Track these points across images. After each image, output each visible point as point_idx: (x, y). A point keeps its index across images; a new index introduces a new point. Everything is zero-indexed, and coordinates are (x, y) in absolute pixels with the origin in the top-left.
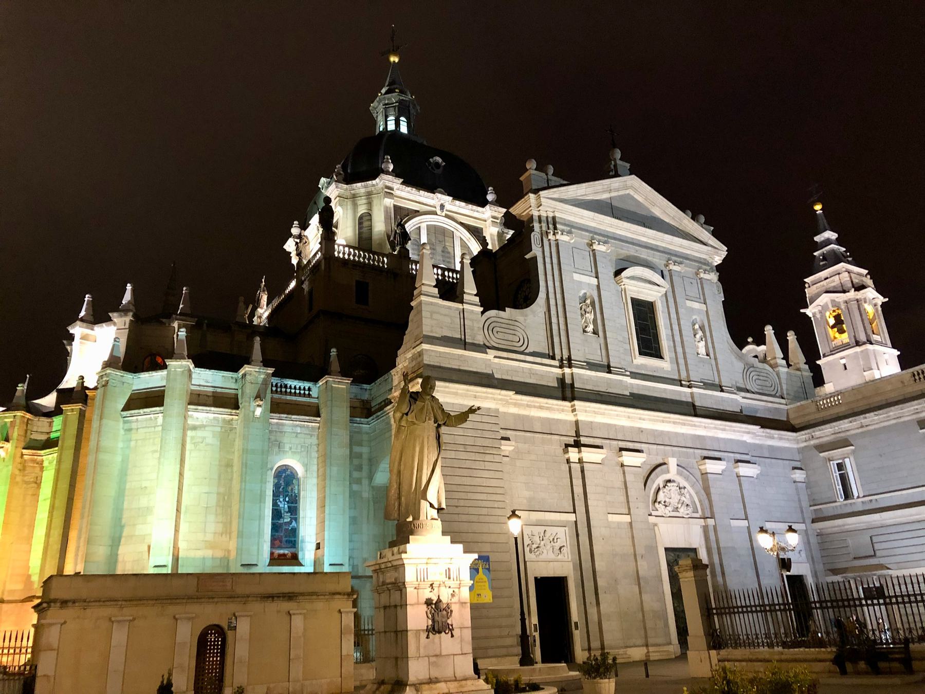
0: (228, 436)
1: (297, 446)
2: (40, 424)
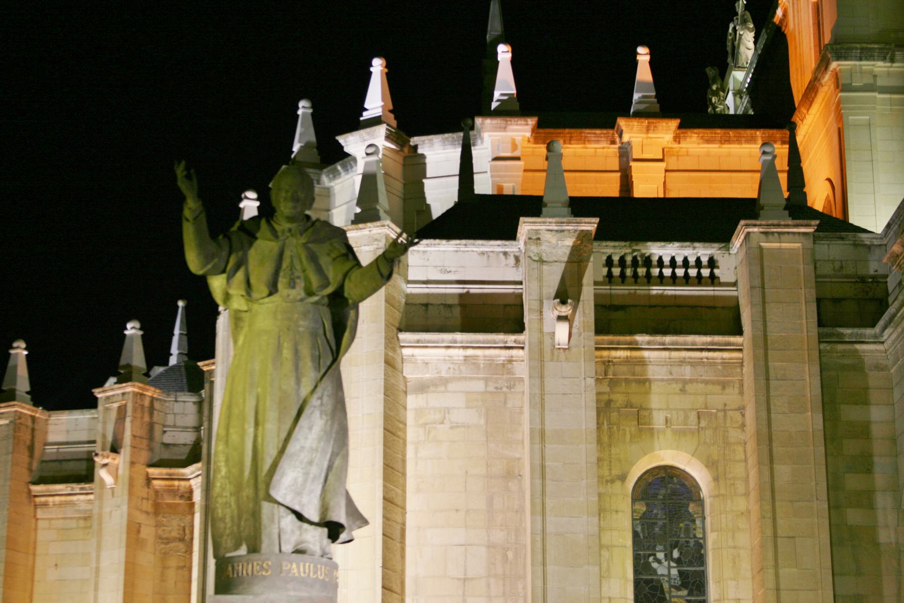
0: (505, 403)
1: (686, 417)
2: (177, 408)
